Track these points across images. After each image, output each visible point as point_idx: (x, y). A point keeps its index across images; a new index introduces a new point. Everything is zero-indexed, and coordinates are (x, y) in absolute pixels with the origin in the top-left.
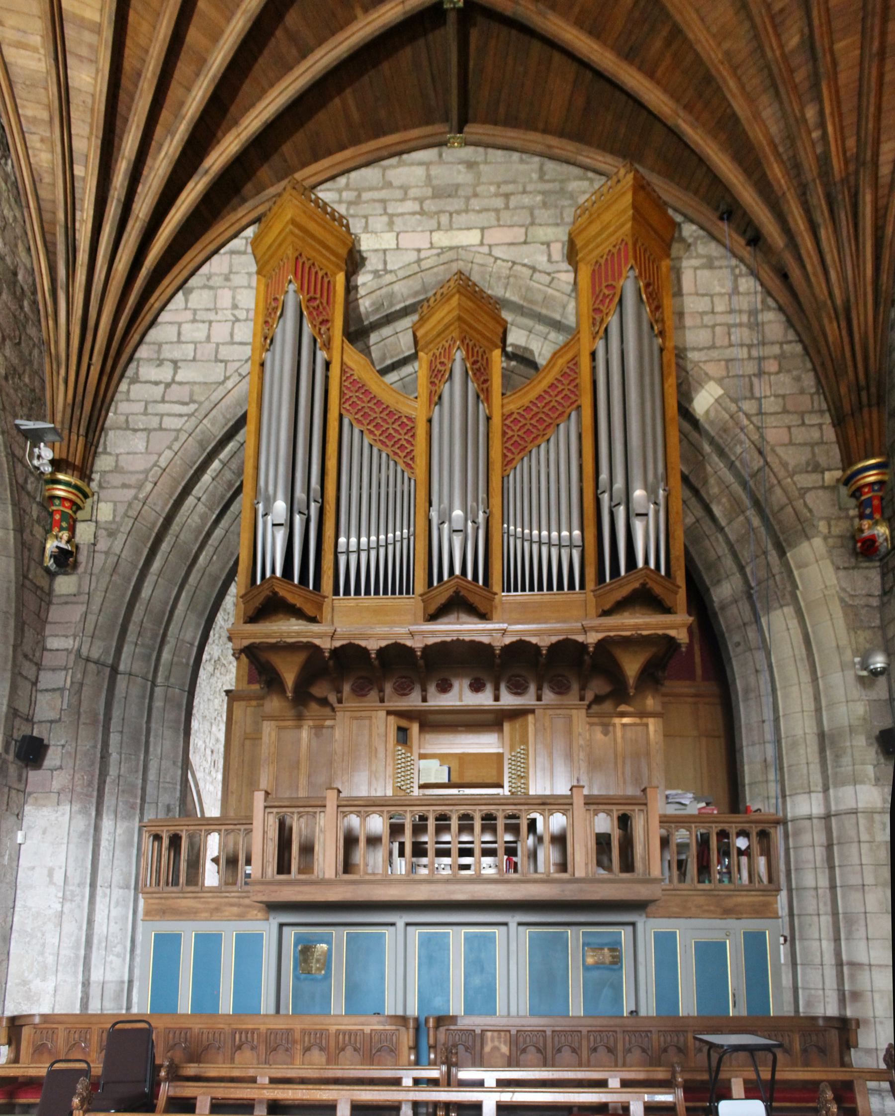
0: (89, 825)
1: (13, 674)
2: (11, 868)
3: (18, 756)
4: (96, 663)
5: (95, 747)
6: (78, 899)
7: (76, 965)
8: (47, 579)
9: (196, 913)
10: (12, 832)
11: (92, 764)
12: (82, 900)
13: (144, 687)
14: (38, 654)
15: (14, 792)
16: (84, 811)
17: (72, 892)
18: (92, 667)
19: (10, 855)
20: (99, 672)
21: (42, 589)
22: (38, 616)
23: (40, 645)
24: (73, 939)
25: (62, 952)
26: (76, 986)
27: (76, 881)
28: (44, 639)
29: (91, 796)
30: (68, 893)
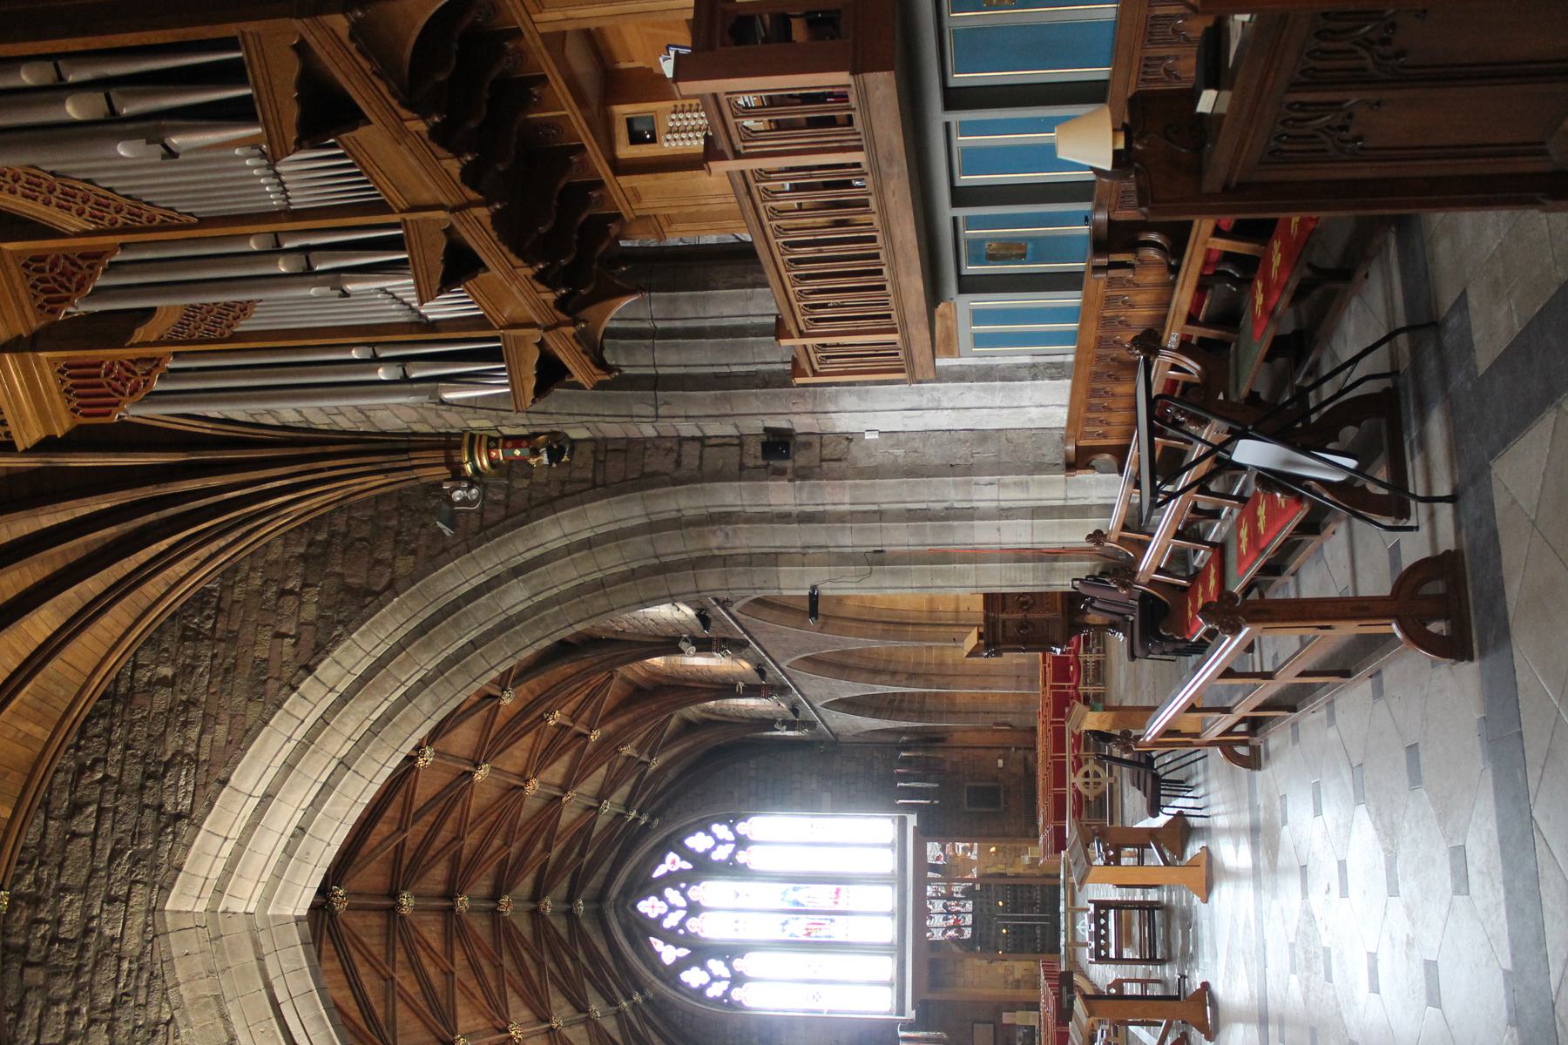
0: (849, 391)
1: (701, 480)
2: (906, 442)
3: (787, 457)
4: (657, 409)
5: (756, 394)
6: (936, 394)
7: (1012, 389)
8: (580, 447)
9: (947, 328)
10: (868, 448)
11: (776, 395)
12: (938, 390)
13: (664, 347)
14: (668, 445)
15: (827, 452)
16: (834, 398)
17: (928, 401)
18: (662, 411)
19: (892, 446)
20: (666, 403)
21: (595, 452)
22: (625, 451)
23: (657, 442)
24: (982, 394)
25: (998, 403)
26: (1036, 386)
27: (917, 398)
28: (647, 439)
29: (815, 392)
30: (931, 405)
